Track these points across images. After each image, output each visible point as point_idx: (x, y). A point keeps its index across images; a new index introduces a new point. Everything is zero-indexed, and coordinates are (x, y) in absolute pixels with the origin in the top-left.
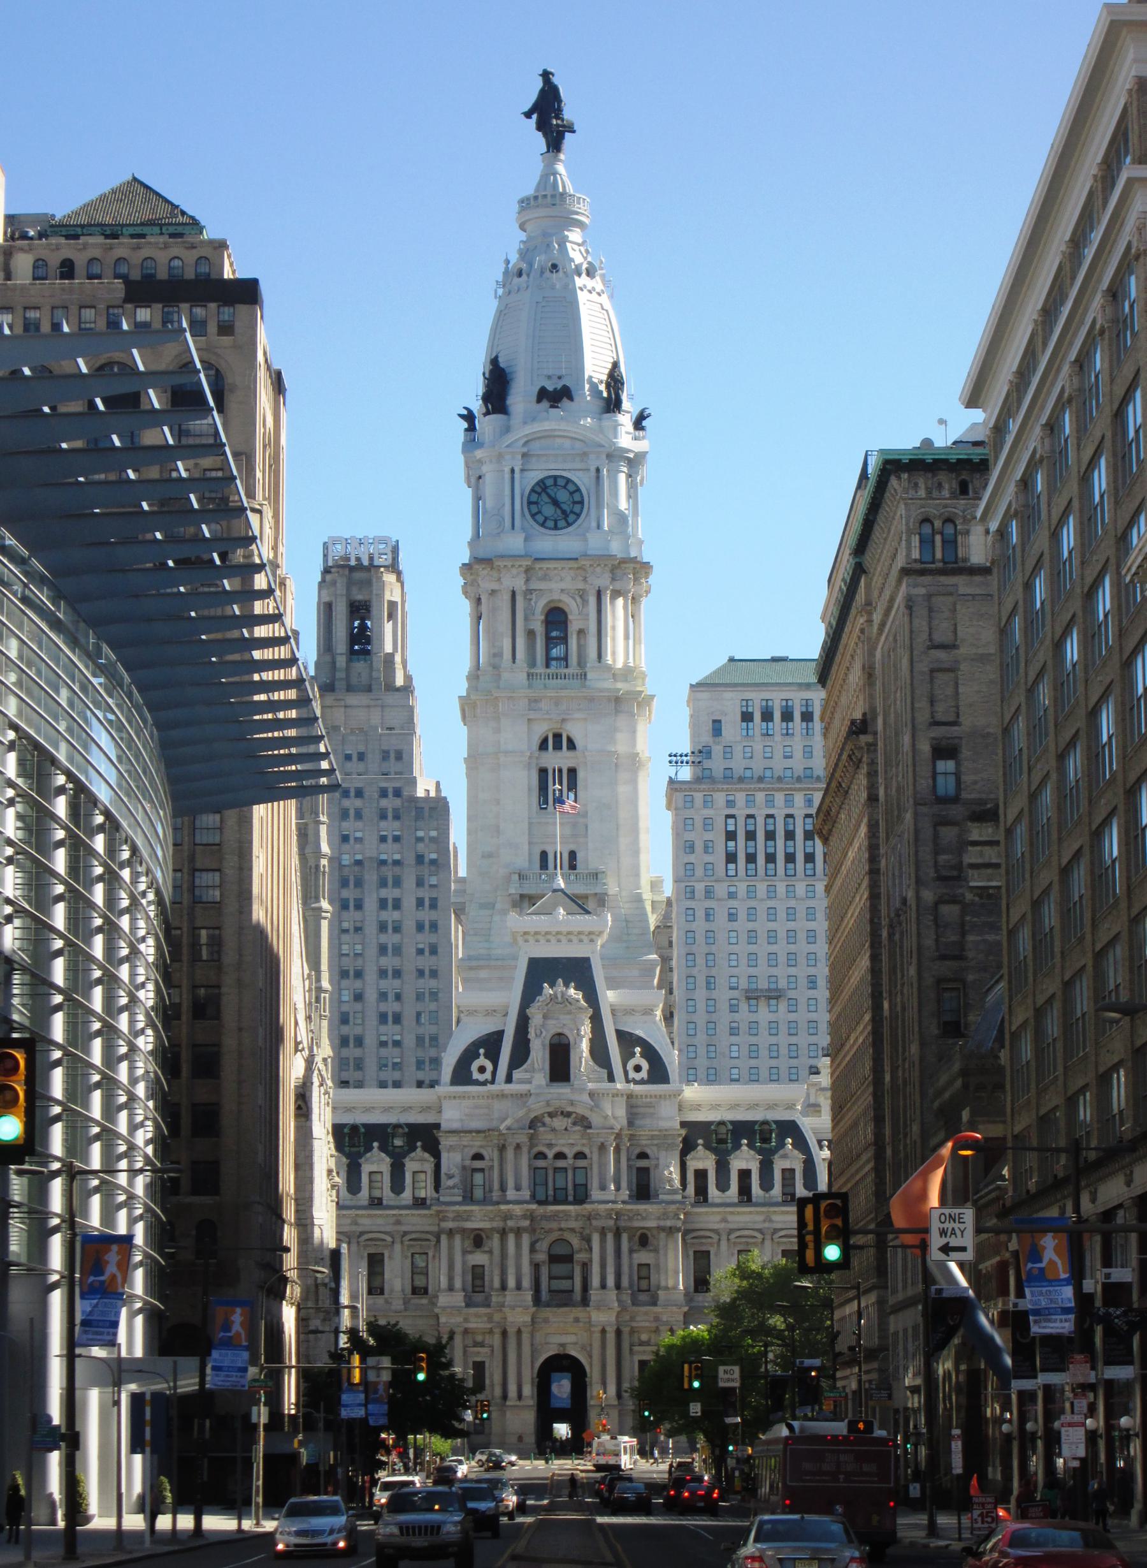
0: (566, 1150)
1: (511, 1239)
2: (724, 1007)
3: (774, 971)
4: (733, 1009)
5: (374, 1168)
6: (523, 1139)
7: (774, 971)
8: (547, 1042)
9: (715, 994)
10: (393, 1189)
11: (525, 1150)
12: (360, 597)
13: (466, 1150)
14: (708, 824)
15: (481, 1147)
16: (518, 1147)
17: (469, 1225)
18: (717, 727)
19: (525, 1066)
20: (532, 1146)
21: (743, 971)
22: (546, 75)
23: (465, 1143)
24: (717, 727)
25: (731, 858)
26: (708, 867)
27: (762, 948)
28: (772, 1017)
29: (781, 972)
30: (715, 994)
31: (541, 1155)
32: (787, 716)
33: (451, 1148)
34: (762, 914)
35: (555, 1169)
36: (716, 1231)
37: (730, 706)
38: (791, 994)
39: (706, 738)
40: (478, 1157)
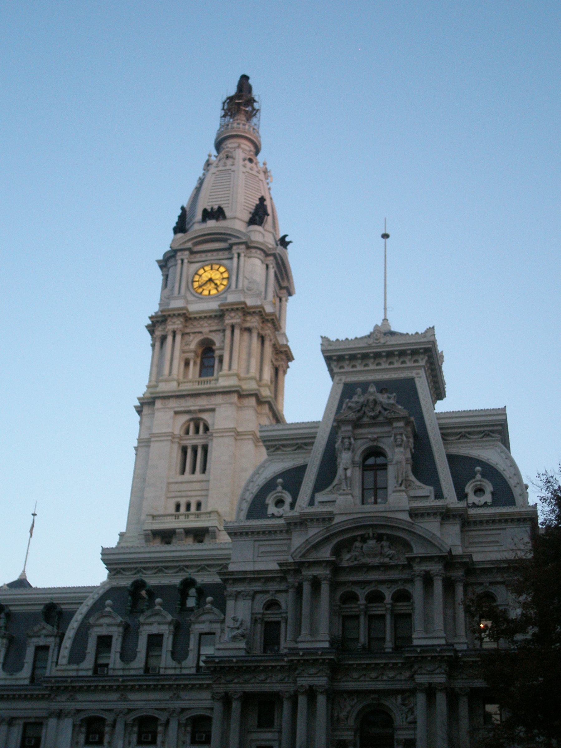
0: (383, 589)
1: (302, 700)
5: (155, 629)
6: (323, 572)
8: (358, 458)
10: (173, 654)
11: (325, 588)
13: (258, 596)
15: (278, 591)
16: (316, 584)
17: (249, 688)
19: (330, 488)
20: (334, 585)
23: (256, 589)
31: (350, 598)
33: (237, 596)
35: (372, 618)
40: (272, 605)
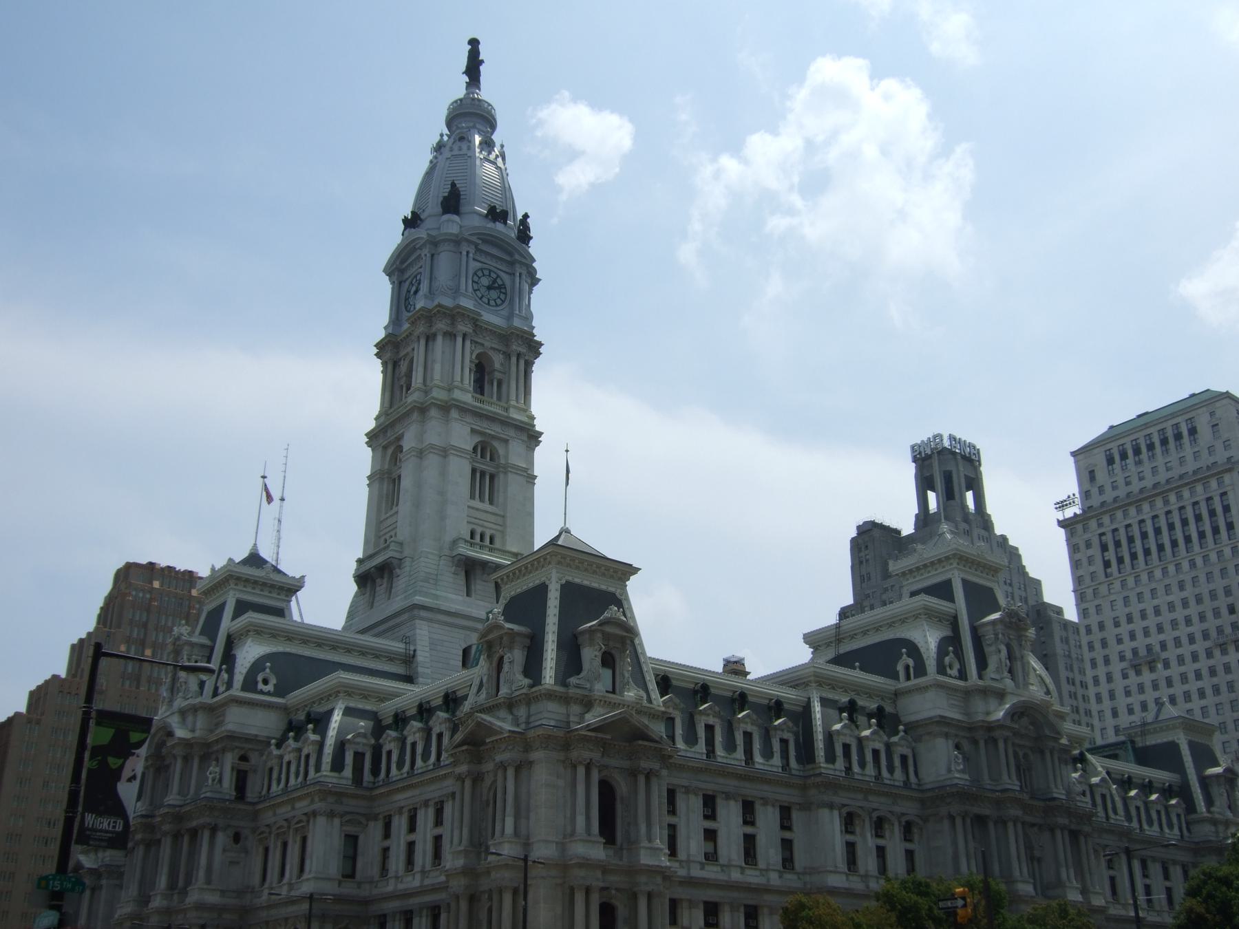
2: (1117, 676)
3: (1148, 641)
4: (1125, 676)
7: (1148, 641)
9: (1111, 668)
12: (928, 475)
14: (1088, 545)
18: (1092, 473)
21: (1127, 646)
22: (474, 43)
24: (1092, 473)
25: (1107, 564)
26: (1093, 575)
27: (1138, 625)
28: (1153, 676)
29: (1154, 640)
30: (1111, 668)
32: (1137, 451)
34: (1134, 599)
36: (267, 826)
37: (1099, 459)
38: (1164, 655)
39: (1087, 486)
